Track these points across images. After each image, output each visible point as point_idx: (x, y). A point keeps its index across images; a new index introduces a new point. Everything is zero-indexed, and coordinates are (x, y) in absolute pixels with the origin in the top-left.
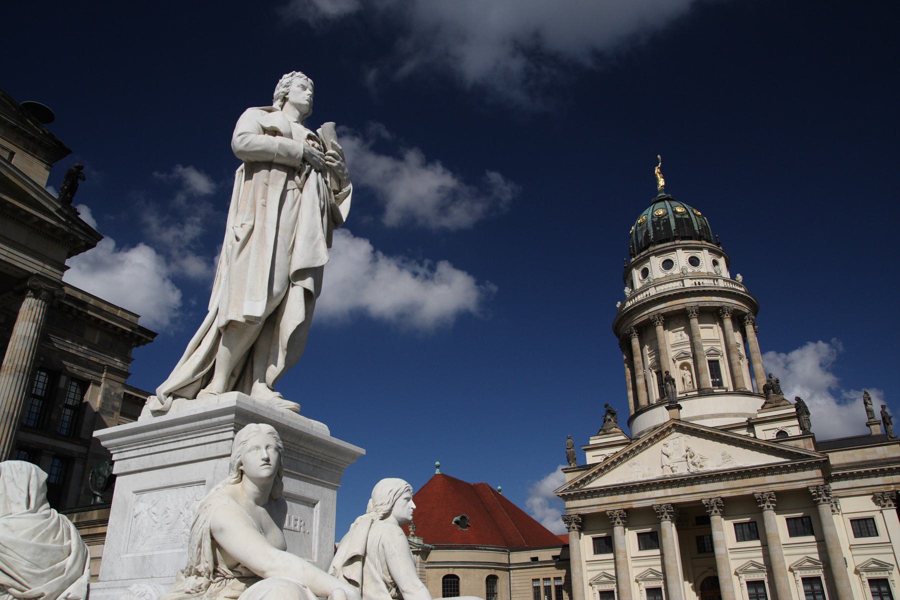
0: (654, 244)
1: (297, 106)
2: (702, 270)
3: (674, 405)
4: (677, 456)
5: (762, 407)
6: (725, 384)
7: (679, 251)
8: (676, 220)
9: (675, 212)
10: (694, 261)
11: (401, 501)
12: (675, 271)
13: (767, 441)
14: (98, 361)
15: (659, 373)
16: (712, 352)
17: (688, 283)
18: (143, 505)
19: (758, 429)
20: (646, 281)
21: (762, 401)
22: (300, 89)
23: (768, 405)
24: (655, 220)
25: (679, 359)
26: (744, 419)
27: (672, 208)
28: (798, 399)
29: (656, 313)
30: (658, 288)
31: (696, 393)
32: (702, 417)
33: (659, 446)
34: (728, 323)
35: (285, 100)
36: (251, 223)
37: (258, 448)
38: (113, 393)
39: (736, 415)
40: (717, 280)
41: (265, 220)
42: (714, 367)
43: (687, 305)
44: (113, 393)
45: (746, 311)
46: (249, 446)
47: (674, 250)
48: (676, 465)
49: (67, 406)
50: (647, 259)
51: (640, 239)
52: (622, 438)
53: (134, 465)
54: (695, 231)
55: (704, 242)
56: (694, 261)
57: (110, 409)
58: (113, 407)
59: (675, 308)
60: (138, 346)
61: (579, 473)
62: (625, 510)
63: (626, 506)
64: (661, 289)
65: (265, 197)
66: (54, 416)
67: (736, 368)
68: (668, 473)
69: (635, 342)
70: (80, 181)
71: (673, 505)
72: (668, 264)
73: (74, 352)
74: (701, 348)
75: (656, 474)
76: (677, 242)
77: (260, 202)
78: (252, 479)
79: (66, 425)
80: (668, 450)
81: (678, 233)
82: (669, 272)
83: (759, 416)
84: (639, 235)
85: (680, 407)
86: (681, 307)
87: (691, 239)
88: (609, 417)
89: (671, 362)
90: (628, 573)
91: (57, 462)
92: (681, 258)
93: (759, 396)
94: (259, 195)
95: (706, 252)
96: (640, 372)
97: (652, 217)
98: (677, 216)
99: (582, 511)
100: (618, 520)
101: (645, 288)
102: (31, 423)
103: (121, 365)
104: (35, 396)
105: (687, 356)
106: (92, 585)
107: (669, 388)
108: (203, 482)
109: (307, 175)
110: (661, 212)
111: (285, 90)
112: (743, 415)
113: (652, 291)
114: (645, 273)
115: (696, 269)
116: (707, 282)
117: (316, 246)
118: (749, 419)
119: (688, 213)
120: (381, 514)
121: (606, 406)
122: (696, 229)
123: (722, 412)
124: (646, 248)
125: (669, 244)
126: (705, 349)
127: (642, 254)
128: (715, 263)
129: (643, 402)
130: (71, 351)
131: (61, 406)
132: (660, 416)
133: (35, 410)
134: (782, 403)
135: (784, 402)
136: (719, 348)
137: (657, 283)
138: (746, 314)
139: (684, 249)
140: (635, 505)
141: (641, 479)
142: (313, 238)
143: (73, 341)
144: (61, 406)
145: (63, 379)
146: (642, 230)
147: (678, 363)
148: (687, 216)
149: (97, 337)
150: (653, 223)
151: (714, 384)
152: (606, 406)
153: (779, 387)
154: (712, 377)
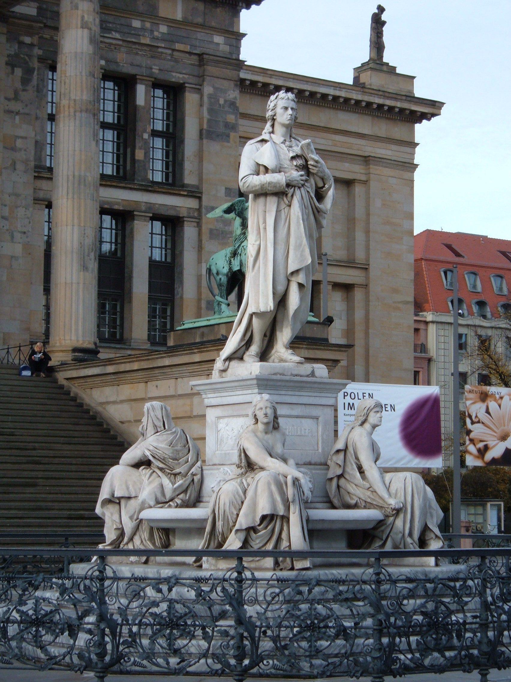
1: (284, 125)
11: (372, 414)
14: (188, 48)
18: (222, 424)
22: (282, 110)
35: (274, 120)
36: (258, 243)
37: (261, 409)
38: (222, 101)
44: (222, 101)
46: (258, 407)
49: (155, 134)
53: (213, 402)
58: (227, 125)
60: (248, 7)
65: (265, 222)
66: (139, 155)
73: (147, 41)
77: (262, 227)
79: (159, 165)
91: (157, 225)
102: (109, 170)
103: (227, 48)
104: (105, 126)
106: (204, 468)
109: (292, 196)
117: (303, 251)
120: (360, 422)
130: (143, 41)
133: (109, 147)
142: (300, 245)
144: (146, 136)
145: (141, 90)
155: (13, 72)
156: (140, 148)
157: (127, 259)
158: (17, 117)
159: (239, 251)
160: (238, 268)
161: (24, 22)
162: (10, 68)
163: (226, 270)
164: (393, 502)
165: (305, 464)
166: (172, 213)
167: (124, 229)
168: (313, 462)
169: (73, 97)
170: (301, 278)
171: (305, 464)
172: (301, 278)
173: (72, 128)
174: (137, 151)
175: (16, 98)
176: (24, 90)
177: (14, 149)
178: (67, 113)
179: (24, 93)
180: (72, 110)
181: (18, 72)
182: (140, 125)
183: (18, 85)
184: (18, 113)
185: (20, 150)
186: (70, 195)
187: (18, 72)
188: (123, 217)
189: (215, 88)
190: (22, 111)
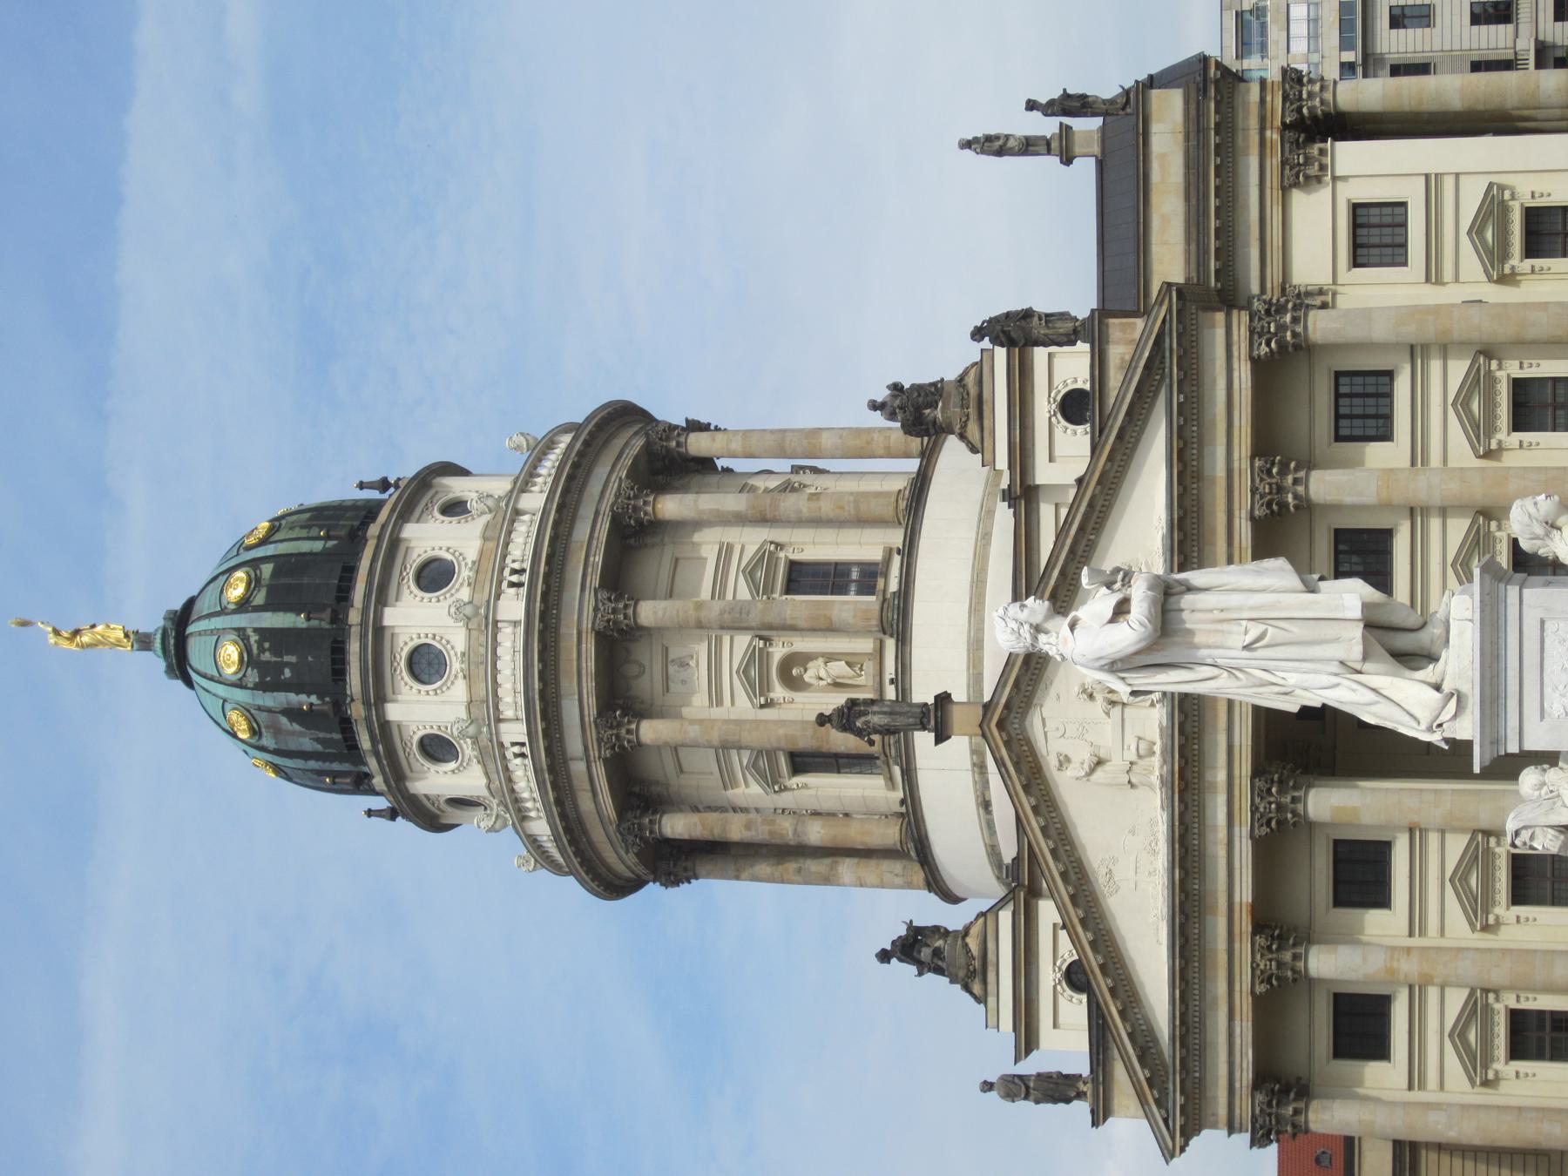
0: (339, 703)
2: (472, 554)
3: (938, 716)
4: (1105, 733)
5: (974, 450)
6: (875, 554)
7: (391, 616)
8: (268, 607)
9: (244, 605)
10: (434, 576)
12: (456, 641)
13: (1095, 448)
15: (803, 762)
16: (760, 575)
17: (513, 606)
19: (1044, 473)
20: (467, 749)
21: (952, 448)
23: (973, 430)
24: (253, 676)
25: (765, 687)
26: (1004, 517)
27: (223, 612)
28: (978, 334)
29: (592, 734)
30: (508, 713)
31: (890, 644)
32: (976, 646)
33: (1068, 786)
34: (670, 506)
39: (984, 538)
40: (518, 513)
41: (1240, 609)
42: (803, 578)
43: (587, 624)
45: (639, 443)
47: (379, 630)
48: (1131, 741)
50: (384, 732)
51: (307, 744)
52: (1005, 917)
54: (324, 553)
55: (373, 530)
56: (434, 576)
59: (590, 665)
61: (1119, 1071)
62: (1258, 927)
63: (1244, 923)
64: (512, 698)
67: (826, 508)
68: (1155, 768)
69: (676, 825)
71: (1257, 772)
72: (426, 664)
74: (740, 608)
75: (1150, 813)
76: (354, 617)
78: (1558, 515)
80: (1081, 756)
81: (322, 608)
82: (455, 665)
83: (1002, 462)
84: (292, 745)
85: (943, 699)
86: (589, 646)
87: (349, 572)
88: (925, 954)
89: (768, 714)
90: (1459, 950)
92: (414, 617)
93: (928, 458)
94: (1209, 616)
95: (410, 531)
96: (786, 827)
97: (239, 685)
98: (260, 598)
99: (1245, 1075)
100: (1287, 956)
101: (493, 755)
105: (756, 662)
107: (877, 720)
108: (1542, 622)
110: (230, 653)
111: (1027, 627)
112: (986, 516)
113: (514, 732)
114: (437, 748)
115: (464, 573)
116: (521, 547)
118: (1009, 496)
119: (254, 563)
121: (884, 956)
122: (318, 546)
123: (965, 576)
124: (346, 725)
125: (354, 647)
126: (744, 593)
127: (365, 743)
128: (455, 508)
129: (889, 834)
132: (947, 771)
134: (973, 391)
135: (971, 380)
136: (751, 550)
137: (486, 709)
138: (647, 446)
139: (382, 601)
140: (1245, 893)
141: (1160, 860)
146: (277, 731)
147: (779, 692)
148: (267, 569)
150: (262, 686)
151: (867, 587)
152: (884, 956)
153: (918, 388)
154: (841, 589)
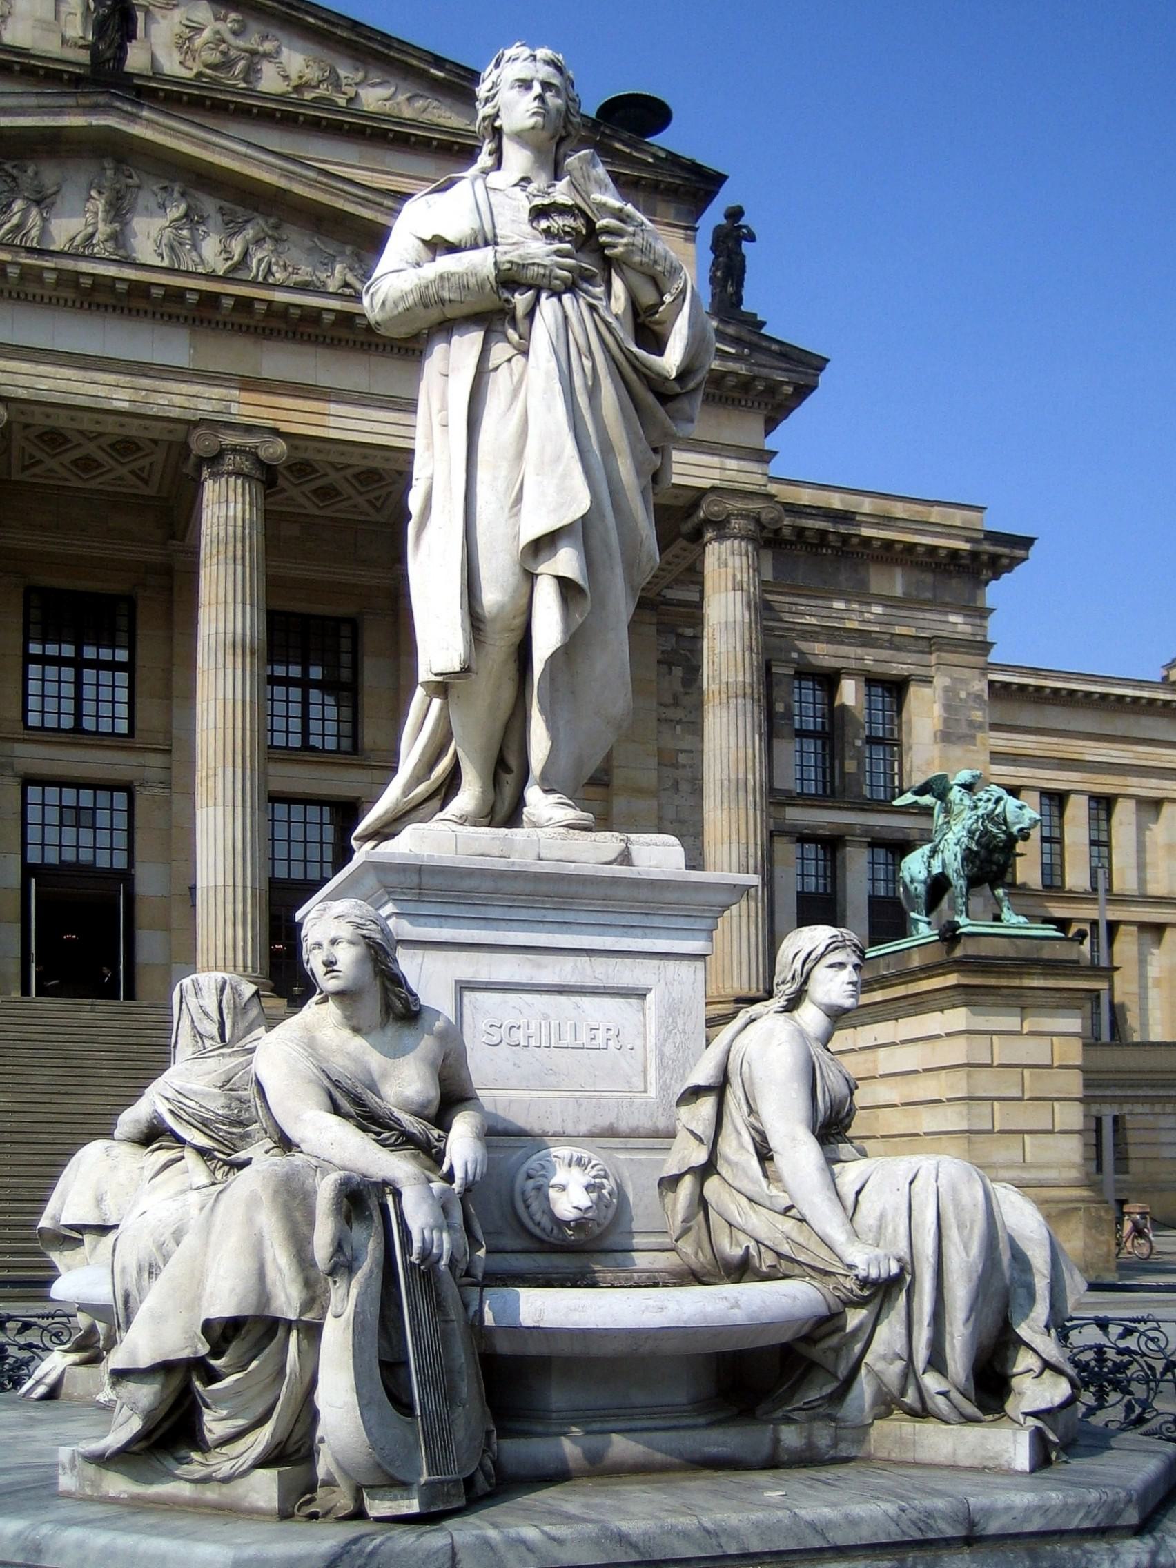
57: (964, 729)
66: (851, 766)
70: (746, 246)
131: (859, 743)
143: (847, 601)
144: (859, 743)
149: (896, 582)
155: (670, 673)
156: (851, 758)
157: (839, 895)
158: (678, 727)
159: (941, 847)
160: (940, 870)
161: (682, 610)
162: (665, 666)
163: (923, 875)
164: (866, 1259)
165: (592, 1135)
166: (899, 836)
167: (833, 860)
168: (623, 1126)
169: (724, 679)
170: (566, 562)
171: (592, 1135)
172: (566, 562)
173: (725, 720)
174: (847, 763)
175: (676, 703)
176: (686, 693)
177: (675, 766)
178: (717, 701)
179: (687, 697)
180: (724, 696)
181: (678, 672)
182: (849, 731)
183: (678, 687)
184: (679, 722)
185: (684, 766)
186: (726, 805)
187: (678, 672)
188: (832, 845)
189: (954, 679)
190: (684, 719)
